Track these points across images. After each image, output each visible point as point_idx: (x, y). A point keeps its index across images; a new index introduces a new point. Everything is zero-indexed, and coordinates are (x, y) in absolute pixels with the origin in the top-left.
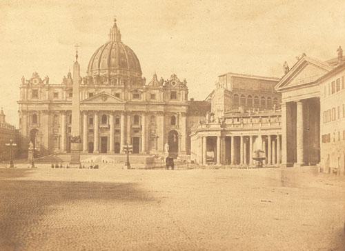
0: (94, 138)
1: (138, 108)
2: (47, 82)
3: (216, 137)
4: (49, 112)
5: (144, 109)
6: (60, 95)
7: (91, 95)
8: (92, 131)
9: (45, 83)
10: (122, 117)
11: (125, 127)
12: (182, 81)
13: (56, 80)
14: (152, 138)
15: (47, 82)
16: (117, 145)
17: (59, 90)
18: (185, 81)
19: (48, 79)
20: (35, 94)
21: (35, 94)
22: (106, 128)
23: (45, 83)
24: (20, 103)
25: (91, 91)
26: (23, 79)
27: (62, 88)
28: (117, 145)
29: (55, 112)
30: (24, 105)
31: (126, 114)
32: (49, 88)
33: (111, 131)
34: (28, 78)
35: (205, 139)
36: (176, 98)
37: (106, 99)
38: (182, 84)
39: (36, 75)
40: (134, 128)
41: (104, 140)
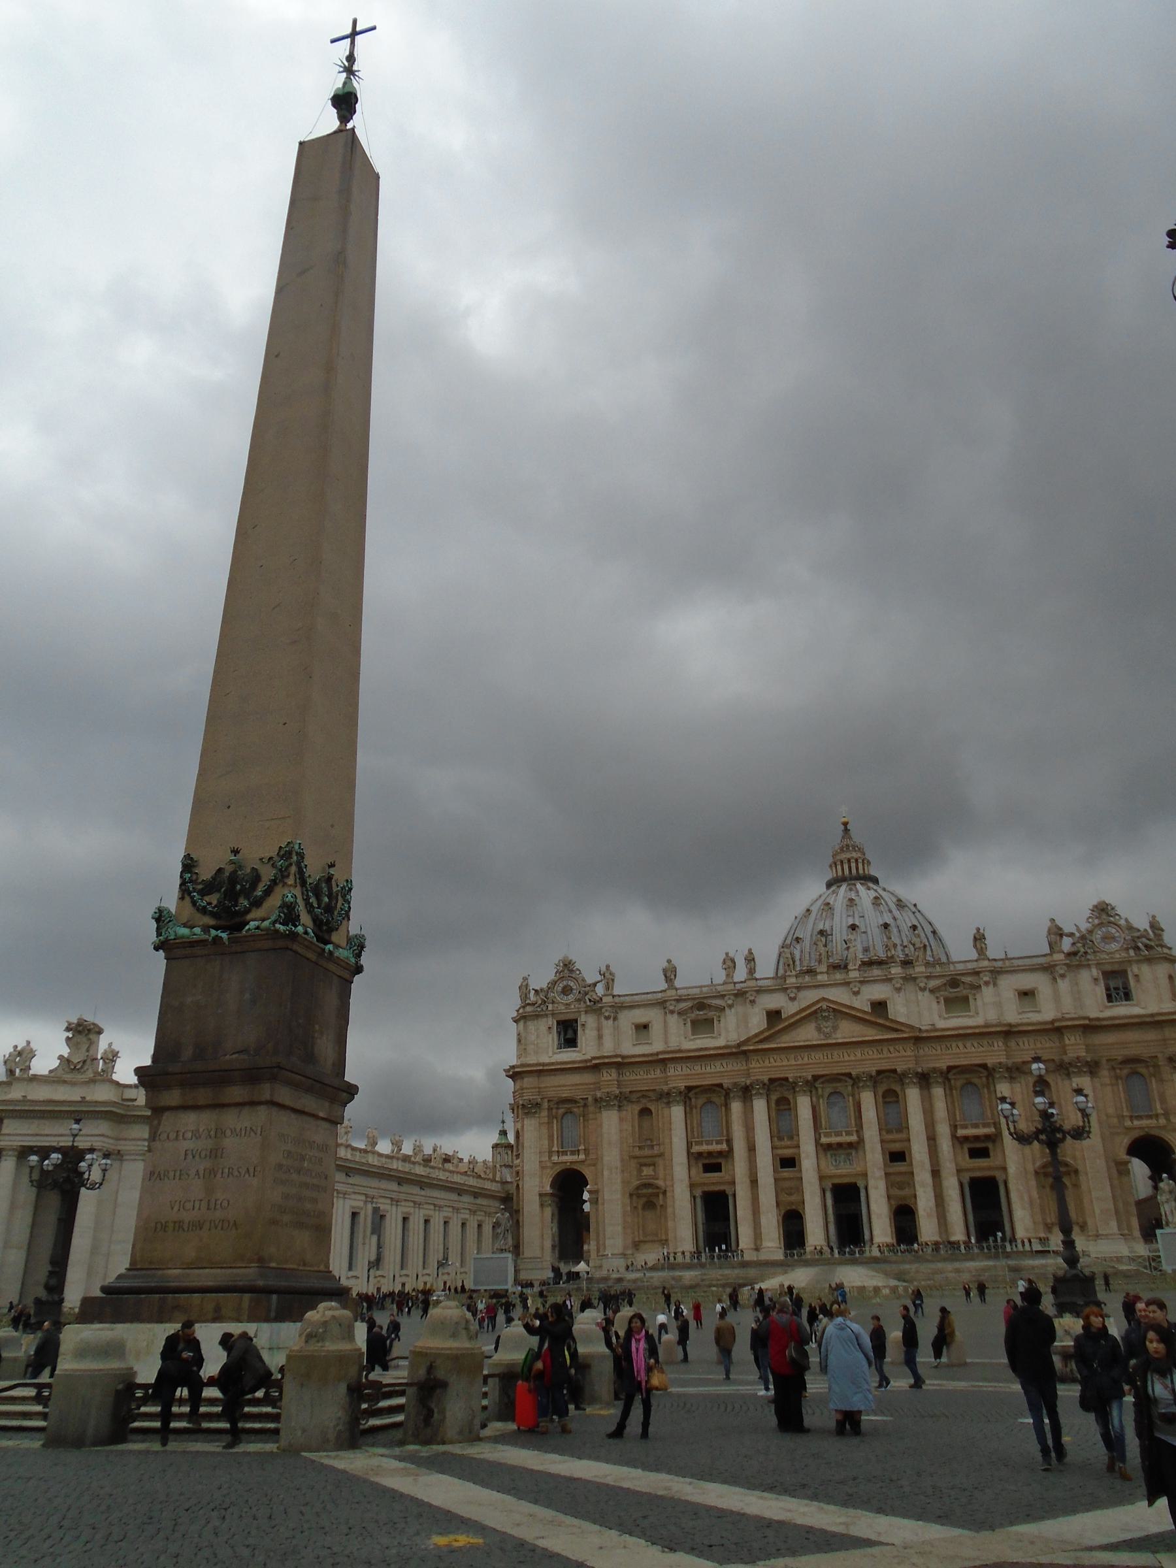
0: (799, 1190)
1: (971, 1054)
2: (608, 988)
4: (621, 1100)
5: (995, 1054)
6: (656, 1029)
7: (774, 1016)
8: (789, 1162)
9: (600, 990)
10: (913, 1096)
11: (932, 1139)
12: (1142, 924)
15: (609, 983)
16: (904, 1218)
17: (652, 1016)
18: (1155, 926)
19: (608, 977)
20: (568, 1033)
21: (568, 1033)
22: (850, 1145)
23: (600, 990)
24: (515, 1074)
26: (524, 988)
27: (662, 1004)
29: (644, 1095)
30: (528, 1081)
31: (924, 1080)
32: (620, 1007)
33: (874, 1156)
34: (542, 978)
36: (1127, 996)
37: (835, 1028)
38: (1145, 935)
39: (567, 968)
40: (966, 1139)
41: (846, 1200)
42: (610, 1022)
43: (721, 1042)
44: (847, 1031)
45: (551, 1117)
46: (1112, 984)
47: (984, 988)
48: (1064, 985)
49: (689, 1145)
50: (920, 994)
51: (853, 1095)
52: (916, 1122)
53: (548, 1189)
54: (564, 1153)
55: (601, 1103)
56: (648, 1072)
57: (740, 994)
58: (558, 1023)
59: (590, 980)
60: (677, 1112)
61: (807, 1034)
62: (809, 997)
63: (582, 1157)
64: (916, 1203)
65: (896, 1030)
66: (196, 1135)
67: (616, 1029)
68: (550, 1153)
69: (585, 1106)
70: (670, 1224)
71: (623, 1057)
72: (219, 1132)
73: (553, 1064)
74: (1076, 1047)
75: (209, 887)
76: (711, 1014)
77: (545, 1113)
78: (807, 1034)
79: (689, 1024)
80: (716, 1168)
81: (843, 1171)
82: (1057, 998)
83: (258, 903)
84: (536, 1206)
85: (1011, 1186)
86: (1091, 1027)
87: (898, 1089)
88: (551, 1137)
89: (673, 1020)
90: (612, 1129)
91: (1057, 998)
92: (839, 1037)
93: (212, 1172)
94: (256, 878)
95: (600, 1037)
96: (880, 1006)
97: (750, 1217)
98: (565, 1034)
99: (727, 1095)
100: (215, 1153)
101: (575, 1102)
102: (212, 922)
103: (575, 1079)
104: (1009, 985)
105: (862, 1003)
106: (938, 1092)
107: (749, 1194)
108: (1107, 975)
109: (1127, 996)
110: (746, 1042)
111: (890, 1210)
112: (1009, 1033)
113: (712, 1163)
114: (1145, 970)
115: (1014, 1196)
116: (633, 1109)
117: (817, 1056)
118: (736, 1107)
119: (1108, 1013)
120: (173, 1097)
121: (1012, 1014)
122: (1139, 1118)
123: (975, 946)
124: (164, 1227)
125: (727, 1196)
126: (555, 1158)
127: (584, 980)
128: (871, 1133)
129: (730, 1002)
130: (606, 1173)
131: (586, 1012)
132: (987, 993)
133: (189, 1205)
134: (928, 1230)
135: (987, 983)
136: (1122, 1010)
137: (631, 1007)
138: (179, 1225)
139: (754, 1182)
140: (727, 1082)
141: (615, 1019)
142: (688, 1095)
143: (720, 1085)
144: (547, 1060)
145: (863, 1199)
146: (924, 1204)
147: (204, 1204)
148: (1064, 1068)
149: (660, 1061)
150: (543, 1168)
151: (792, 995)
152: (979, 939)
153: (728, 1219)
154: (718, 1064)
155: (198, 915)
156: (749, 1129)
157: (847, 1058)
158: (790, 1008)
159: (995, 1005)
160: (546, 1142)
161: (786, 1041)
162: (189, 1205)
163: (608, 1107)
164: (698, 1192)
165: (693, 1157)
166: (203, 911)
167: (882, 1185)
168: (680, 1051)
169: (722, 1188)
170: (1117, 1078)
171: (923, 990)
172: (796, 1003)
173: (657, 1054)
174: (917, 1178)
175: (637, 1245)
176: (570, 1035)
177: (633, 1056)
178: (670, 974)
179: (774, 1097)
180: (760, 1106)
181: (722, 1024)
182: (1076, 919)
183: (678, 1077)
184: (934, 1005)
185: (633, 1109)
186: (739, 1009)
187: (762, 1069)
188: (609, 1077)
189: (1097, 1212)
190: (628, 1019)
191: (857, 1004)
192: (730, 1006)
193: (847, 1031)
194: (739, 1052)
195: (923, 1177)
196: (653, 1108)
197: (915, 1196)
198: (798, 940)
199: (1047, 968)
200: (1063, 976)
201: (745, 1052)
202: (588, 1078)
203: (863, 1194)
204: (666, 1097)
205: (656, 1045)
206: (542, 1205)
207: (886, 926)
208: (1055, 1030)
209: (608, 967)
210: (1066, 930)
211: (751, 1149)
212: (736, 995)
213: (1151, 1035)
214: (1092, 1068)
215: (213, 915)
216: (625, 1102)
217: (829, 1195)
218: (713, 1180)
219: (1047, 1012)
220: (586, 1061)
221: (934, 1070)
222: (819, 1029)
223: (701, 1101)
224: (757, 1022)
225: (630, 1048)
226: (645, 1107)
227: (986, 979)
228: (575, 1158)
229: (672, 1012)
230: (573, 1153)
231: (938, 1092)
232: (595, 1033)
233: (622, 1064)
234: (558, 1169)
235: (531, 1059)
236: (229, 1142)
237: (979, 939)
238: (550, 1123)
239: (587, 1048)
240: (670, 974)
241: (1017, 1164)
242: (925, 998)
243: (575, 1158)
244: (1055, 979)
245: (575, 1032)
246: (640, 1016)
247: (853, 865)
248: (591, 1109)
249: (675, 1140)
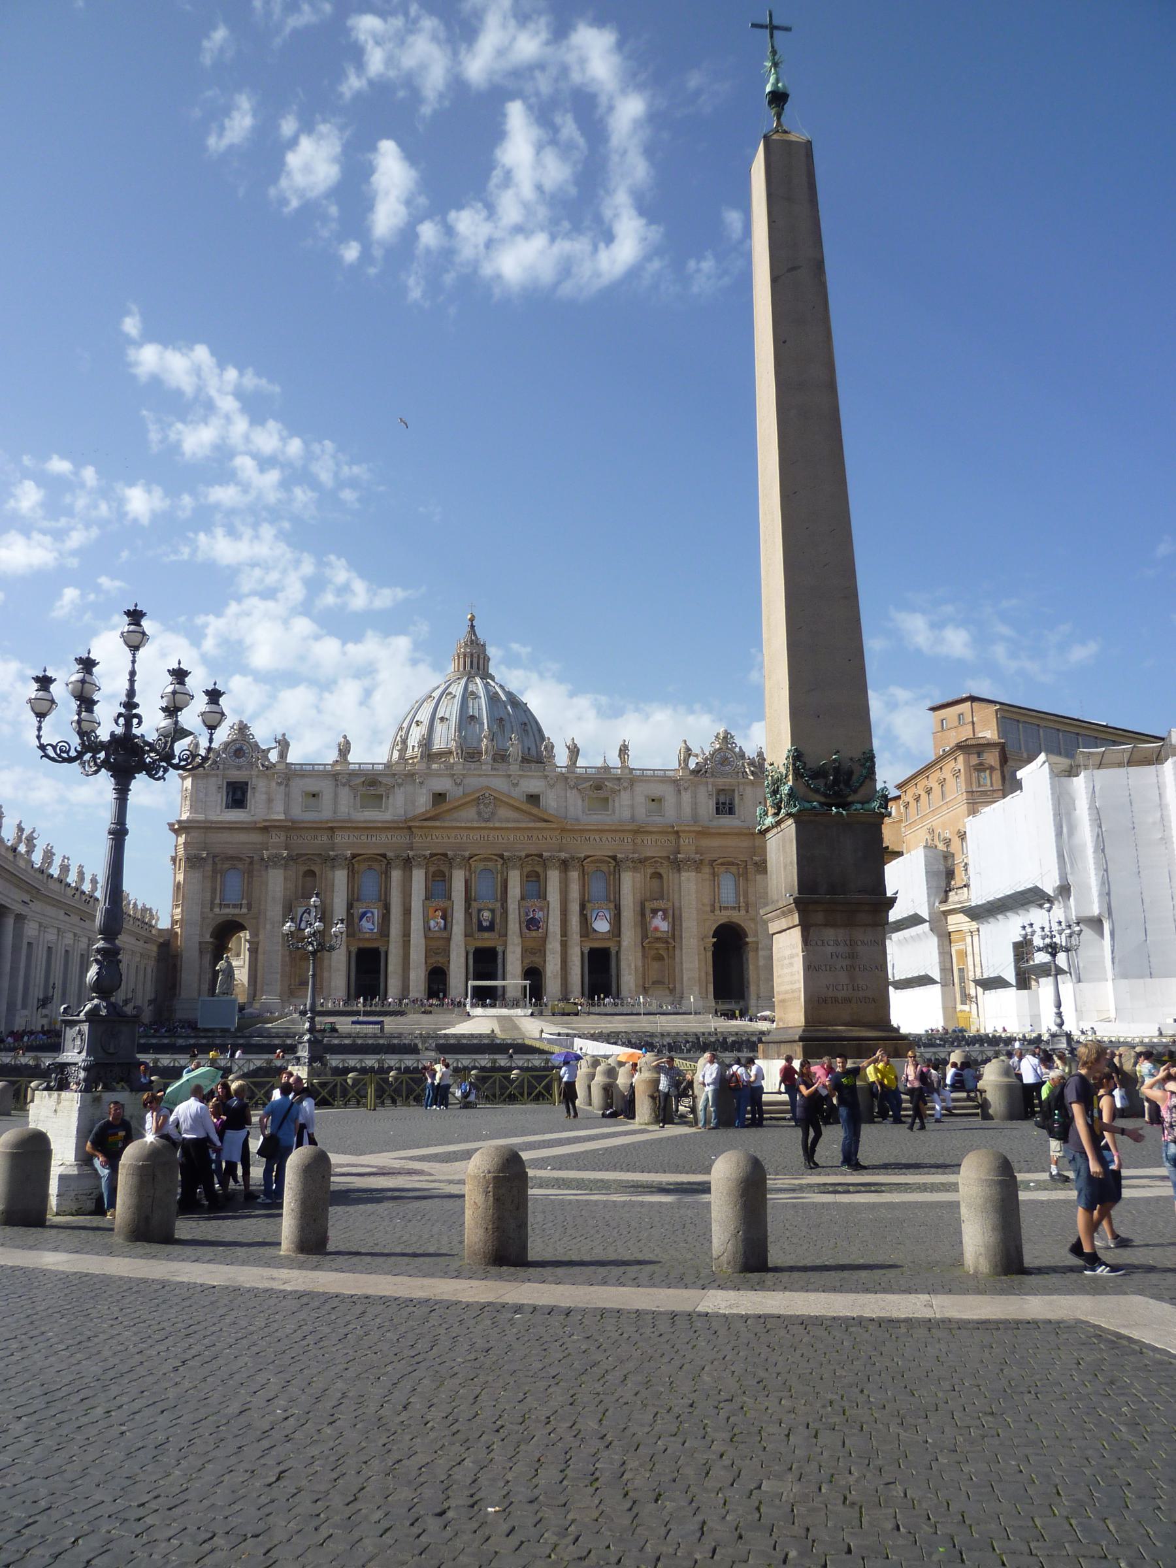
1: (603, 848)
5: (623, 848)
7: (439, 798)
9: (273, 756)
10: (553, 878)
13: (310, 749)
15: (283, 755)
16: (534, 975)
18: (760, 754)
19: (283, 745)
20: (237, 795)
21: (237, 795)
23: (273, 756)
24: (180, 828)
28: (534, 975)
30: (194, 834)
31: (565, 865)
32: (290, 774)
36: (731, 811)
37: (493, 814)
42: (283, 787)
45: (214, 871)
46: (722, 800)
47: (622, 792)
50: (569, 791)
51: (502, 873)
52: (554, 897)
53: (208, 938)
54: (228, 906)
56: (315, 838)
57: (411, 775)
58: (229, 784)
59: (263, 747)
60: (340, 877)
62: (473, 782)
63: (244, 910)
64: (544, 966)
65: (546, 821)
66: (836, 943)
67: (287, 795)
68: (212, 903)
69: (251, 863)
70: (326, 974)
71: (293, 822)
72: (852, 943)
73: (221, 822)
75: (818, 774)
76: (381, 790)
77: (209, 868)
79: (358, 798)
82: (679, 805)
83: (855, 792)
84: (196, 954)
85: (623, 957)
86: (704, 833)
87: (539, 869)
88: (214, 891)
89: (344, 792)
91: (679, 805)
93: (852, 967)
94: (850, 773)
95: (270, 801)
96: (534, 799)
97: (400, 971)
98: (234, 794)
99: (389, 863)
100: (853, 956)
101: (240, 859)
102: (823, 800)
103: (242, 837)
104: (641, 790)
106: (574, 875)
107: (401, 952)
108: (720, 792)
109: (731, 811)
110: (414, 819)
111: (523, 967)
115: (623, 965)
118: (396, 875)
119: (715, 823)
120: (819, 917)
122: (726, 908)
123: (620, 755)
124: (825, 1001)
125: (379, 953)
126: (217, 910)
127: (256, 745)
129: (400, 781)
130: (268, 926)
131: (258, 776)
132: (625, 797)
133: (840, 987)
134: (552, 986)
135: (625, 789)
136: (726, 821)
137: (303, 776)
138: (835, 1000)
140: (390, 854)
141: (287, 785)
142: (352, 863)
143: (384, 856)
144: (214, 818)
145: (500, 961)
146: (552, 967)
147: (850, 986)
148: (677, 865)
150: (203, 918)
151: (458, 781)
152: (624, 750)
153: (378, 972)
154: (383, 836)
155: (811, 794)
157: (501, 840)
159: (626, 807)
160: (209, 894)
162: (840, 987)
163: (275, 866)
164: (354, 949)
166: (817, 791)
167: (519, 950)
168: (350, 821)
169: (375, 945)
170: (714, 874)
171: (572, 788)
172: (461, 788)
173: (327, 822)
174: (549, 946)
176: (239, 795)
177: (303, 822)
178: (344, 749)
179: (432, 869)
180: (419, 876)
181: (391, 800)
182: (704, 744)
183: (345, 843)
184: (580, 802)
187: (426, 843)
188: (277, 838)
189: (685, 979)
191: (514, 794)
192: (400, 785)
194: (407, 827)
195: (554, 946)
196: (316, 869)
197: (545, 961)
198: (418, 724)
200: (686, 789)
201: (410, 828)
202: (255, 837)
203: (500, 956)
204: (332, 862)
205: (325, 813)
206: (201, 952)
207: (501, 719)
209: (284, 735)
210: (695, 750)
211: (407, 912)
212: (406, 775)
214: (698, 866)
215: (825, 795)
216: (291, 863)
217: (471, 957)
220: (255, 823)
221: (573, 858)
222: (479, 813)
223: (364, 866)
224: (423, 802)
227: (625, 784)
228: (237, 911)
229: (344, 785)
230: (235, 906)
231: (574, 875)
232: (264, 797)
233: (291, 827)
234: (220, 920)
235: (201, 817)
236: (860, 949)
237: (624, 750)
238: (214, 878)
239: (258, 808)
240: (344, 749)
242: (573, 797)
243: (237, 911)
244: (679, 791)
245: (244, 793)
246: (312, 785)
247: (475, 660)
248: (256, 867)
249: (336, 900)
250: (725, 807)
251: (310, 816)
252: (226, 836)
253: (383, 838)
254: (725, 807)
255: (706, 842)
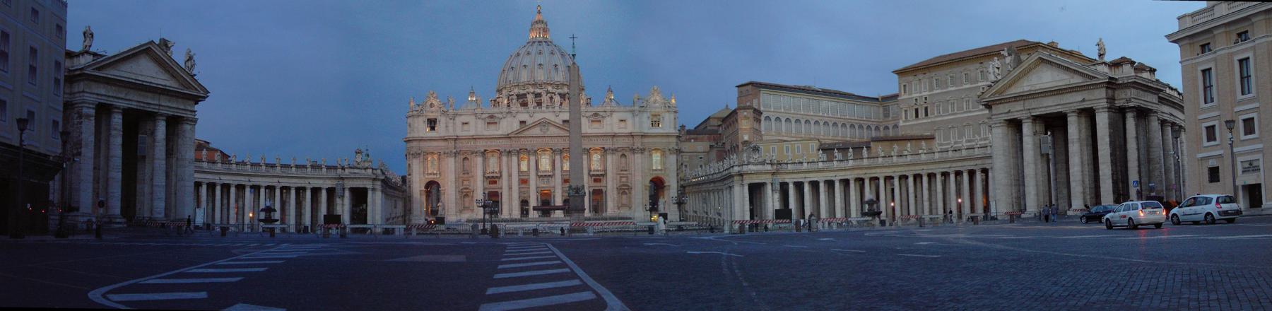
3: (763, 184)
7: (523, 122)
8: (524, 181)
14: (624, 189)
17: (471, 119)
21: (432, 124)
25: (524, 117)
35: (746, 188)
43: (500, 132)
44: (553, 131)
48: (637, 119)
49: (484, 173)
55: (447, 154)
60: (479, 160)
61: (536, 131)
62: (538, 116)
74: (638, 143)
78: (536, 131)
80: (495, 182)
81: (544, 184)
86: (644, 136)
90: (451, 164)
92: (548, 133)
104: (616, 117)
105: (559, 121)
112: (614, 136)
113: (493, 180)
114: (667, 115)
116: (461, 157)
117: (540, 140)
118: (504, 159)
121: (616, 130)
128: (558, 172)
139: (510, 188)
148: (633, 151)
149: (474, 138)
156: (509, 168)
158: (530, 121)
161: (527, 133)
165: (485, 178)
175: (461, 212)
183: (481, 146)
185: (461, 157)
186: (509, 119)
187: (516, 145)
190: (459, 120)
193: (553, 131)
194: (508, 137)
199: (632, 112)
202: (443, 144)
205: (471, 131)
208: (631, 135)
211: (510, 175)
213: (665, 140)
214: (642, 151)
218: (493, 187)
219: (629, 129)
224: (516, 126)
225: (459, 133)
226: (464, 156)
233: (456, 139)
239: (441, 130)
241: (610, 186)
246: (464, 119)
250: (655, 123)
251: (465, 133)
252: (428, 144)
253: (498, 142)
254: (655, 123)
255: (646, 140)
